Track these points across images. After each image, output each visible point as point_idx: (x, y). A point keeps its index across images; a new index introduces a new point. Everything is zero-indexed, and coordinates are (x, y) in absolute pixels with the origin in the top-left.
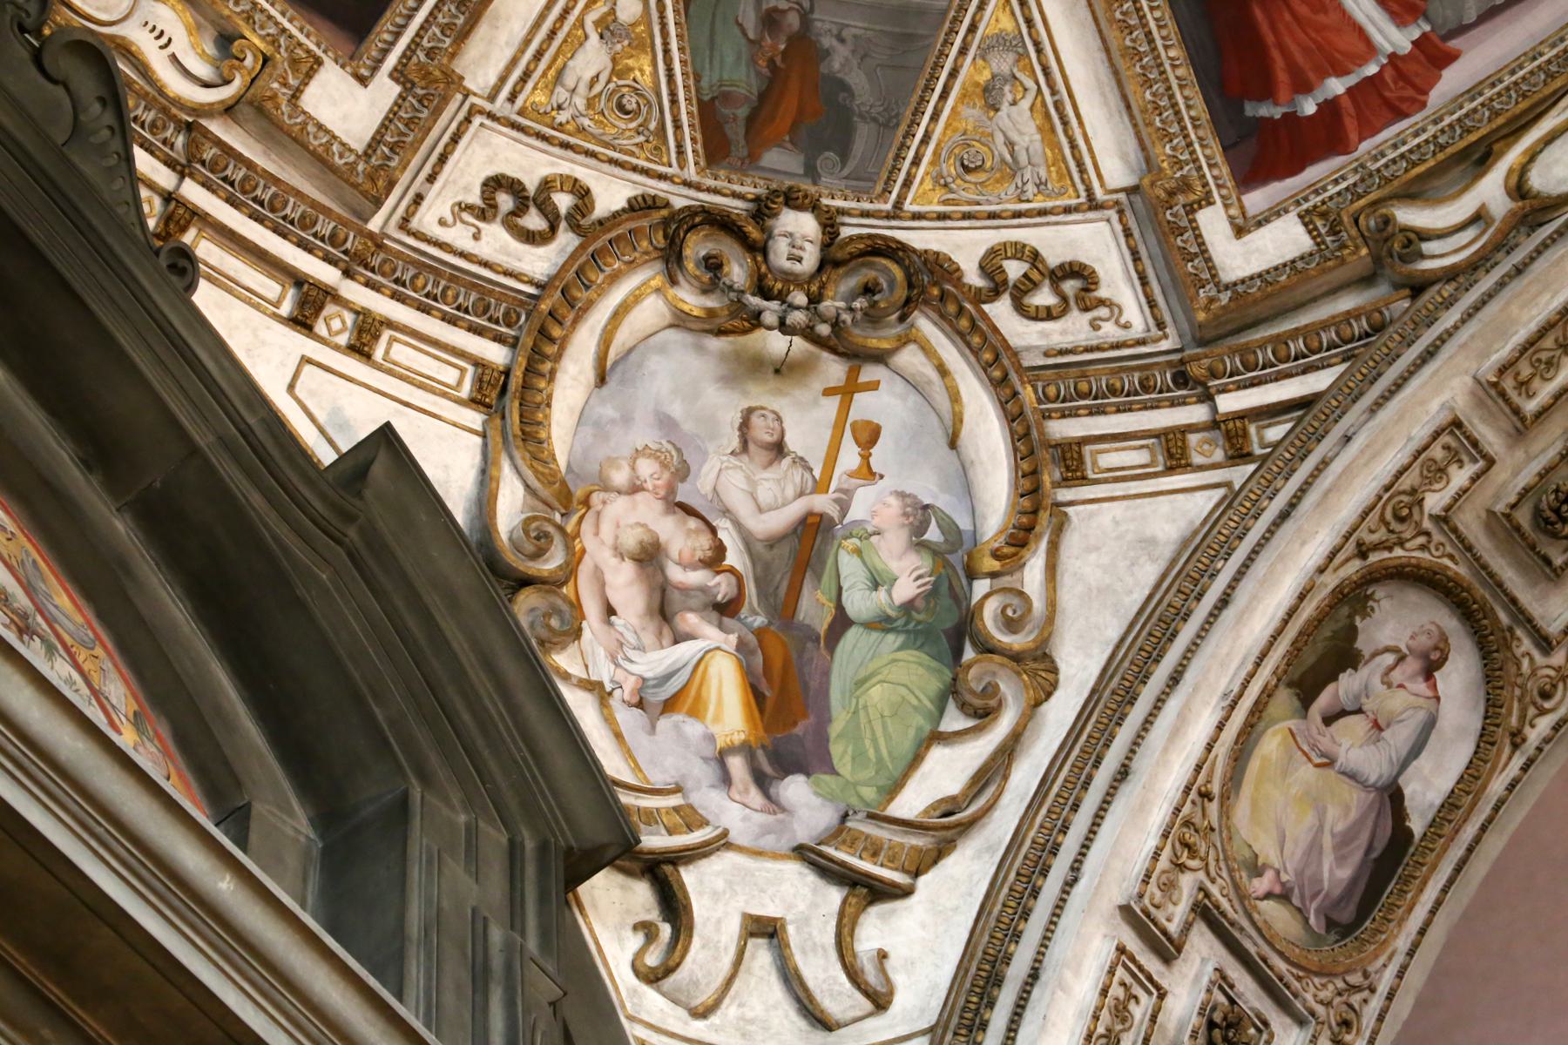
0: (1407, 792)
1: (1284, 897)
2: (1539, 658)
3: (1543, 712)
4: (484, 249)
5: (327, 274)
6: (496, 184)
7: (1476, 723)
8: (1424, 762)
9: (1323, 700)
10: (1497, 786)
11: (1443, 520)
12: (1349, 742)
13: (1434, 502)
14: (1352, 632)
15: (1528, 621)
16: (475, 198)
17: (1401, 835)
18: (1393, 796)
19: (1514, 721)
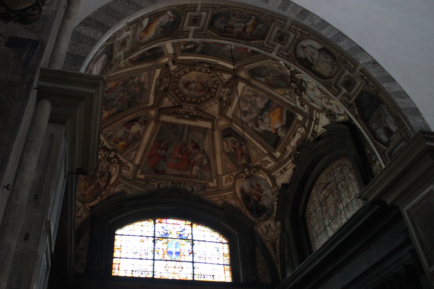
0: (319, 48)
1: (333, 68)
2: (298, 35)
3: (304, 33)
4: (307, 108)
5: (313, 122)
6: (302, 106)
7: (308, 40)
8: (315, 46)
9: (311, 61)
10: (314, 37)
11: (287, 53)
12: (316, 57)
13: (286, 54)
14: (303, 59)
15: (295, 37)
16: (303, 108)
17: (324, 49)
18: (320, 50)
19: (307, 36)
